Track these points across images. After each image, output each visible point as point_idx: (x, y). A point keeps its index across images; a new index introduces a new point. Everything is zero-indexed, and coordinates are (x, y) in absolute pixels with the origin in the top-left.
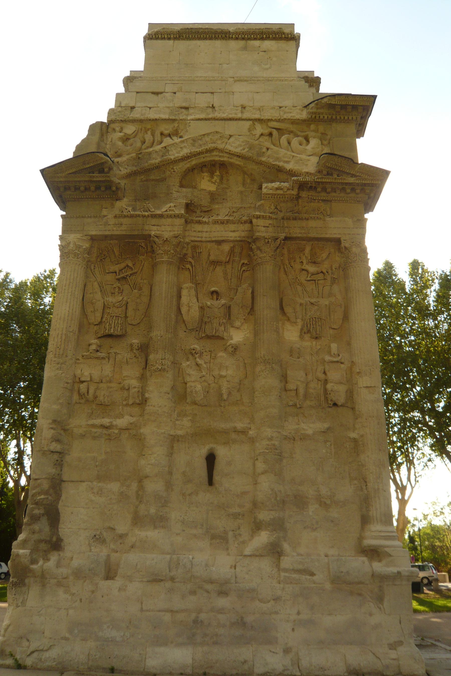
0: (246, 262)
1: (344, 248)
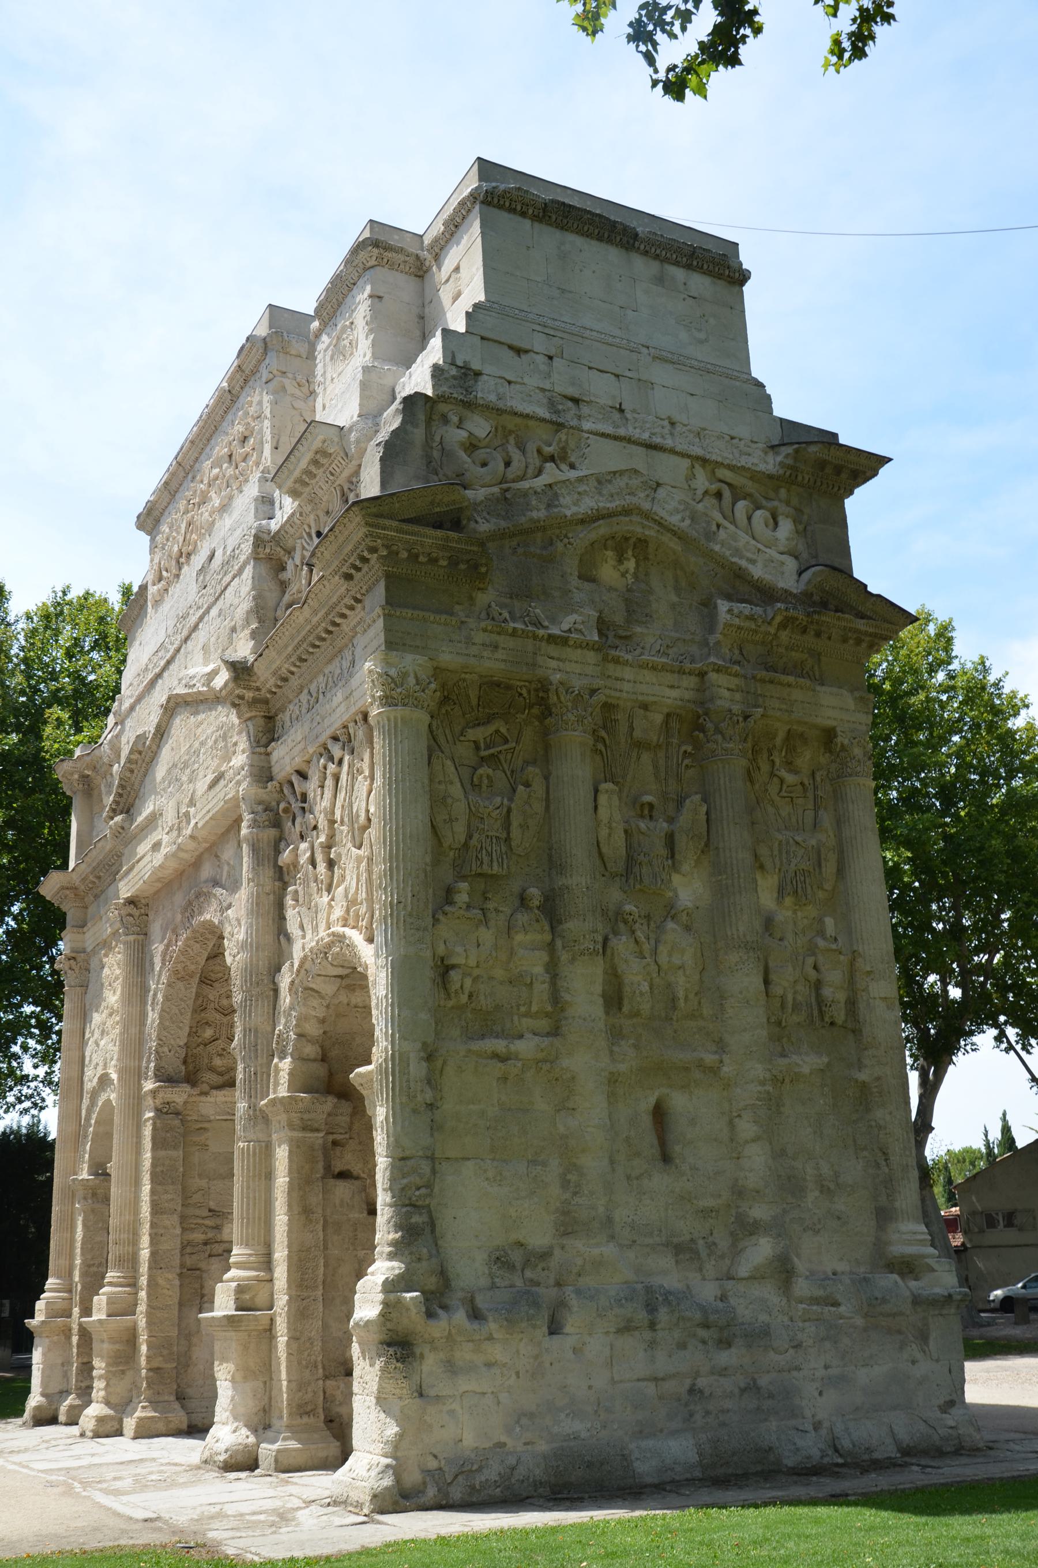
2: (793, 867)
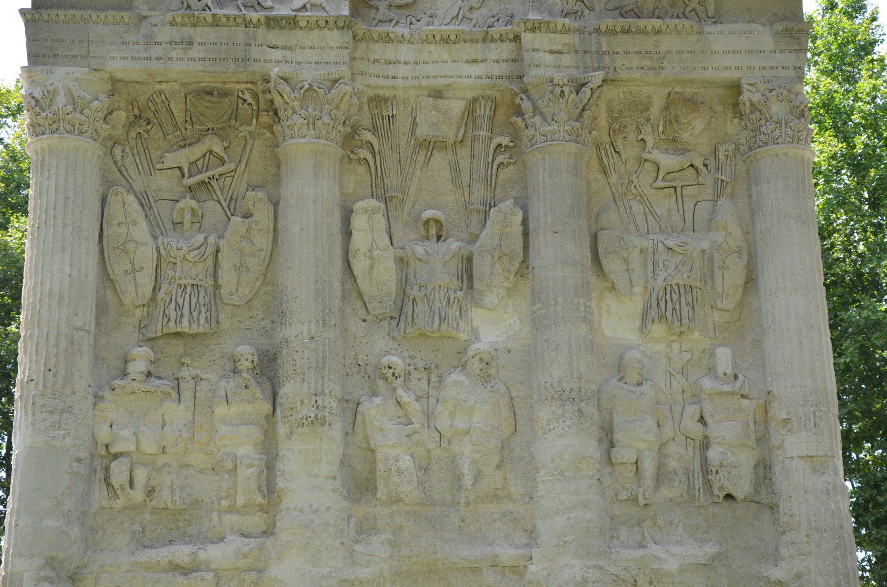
0: (505, 141)
1: (748, 104)
2: (660, 283)
